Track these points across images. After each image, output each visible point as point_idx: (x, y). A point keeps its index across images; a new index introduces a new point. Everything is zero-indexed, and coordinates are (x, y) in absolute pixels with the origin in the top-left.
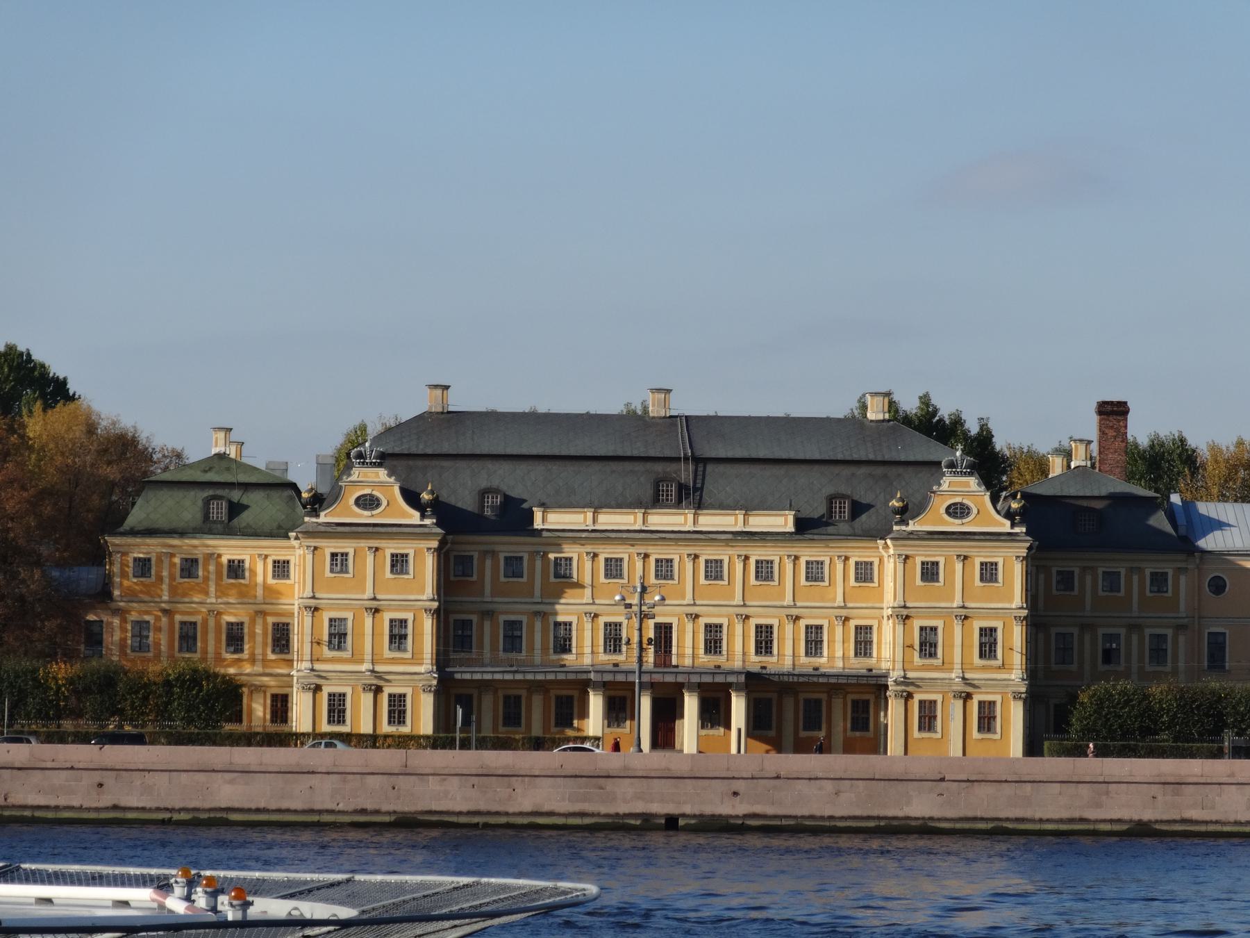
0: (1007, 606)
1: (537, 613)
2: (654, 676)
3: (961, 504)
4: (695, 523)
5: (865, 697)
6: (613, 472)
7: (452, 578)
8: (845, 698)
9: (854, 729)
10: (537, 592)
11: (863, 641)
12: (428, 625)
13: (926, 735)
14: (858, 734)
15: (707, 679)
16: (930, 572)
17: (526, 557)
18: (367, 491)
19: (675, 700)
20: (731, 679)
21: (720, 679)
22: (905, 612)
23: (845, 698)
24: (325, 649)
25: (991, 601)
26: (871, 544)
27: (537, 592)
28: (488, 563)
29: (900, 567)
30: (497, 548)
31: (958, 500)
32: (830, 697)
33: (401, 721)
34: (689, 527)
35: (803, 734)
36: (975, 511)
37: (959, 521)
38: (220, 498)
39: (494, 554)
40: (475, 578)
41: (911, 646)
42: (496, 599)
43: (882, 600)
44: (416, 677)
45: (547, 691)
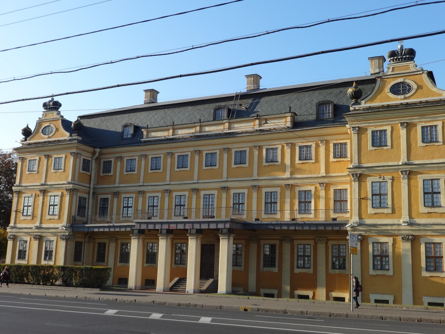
1: (140, 192)
2: (171, 225)
7: (101, 174)
8: (327, 244)
11: (340, 201)
14: (337, 271)
16: (379, 140)
19: (213, 245)
20: (221, 226)
22: (359, 171)
23: (327, 244)
25: (433, 158)
27: (142, 180)
28: (119, 163)
30: (123, 155)
31: (400, 80)
32: (316, 244)
33: (50, 259)
35: (297, 271)
36: (415, 87)
37: (402, 97)
39: (121, 158)
40: (112, 173)
41: (366, 199)
42: (121, 185)
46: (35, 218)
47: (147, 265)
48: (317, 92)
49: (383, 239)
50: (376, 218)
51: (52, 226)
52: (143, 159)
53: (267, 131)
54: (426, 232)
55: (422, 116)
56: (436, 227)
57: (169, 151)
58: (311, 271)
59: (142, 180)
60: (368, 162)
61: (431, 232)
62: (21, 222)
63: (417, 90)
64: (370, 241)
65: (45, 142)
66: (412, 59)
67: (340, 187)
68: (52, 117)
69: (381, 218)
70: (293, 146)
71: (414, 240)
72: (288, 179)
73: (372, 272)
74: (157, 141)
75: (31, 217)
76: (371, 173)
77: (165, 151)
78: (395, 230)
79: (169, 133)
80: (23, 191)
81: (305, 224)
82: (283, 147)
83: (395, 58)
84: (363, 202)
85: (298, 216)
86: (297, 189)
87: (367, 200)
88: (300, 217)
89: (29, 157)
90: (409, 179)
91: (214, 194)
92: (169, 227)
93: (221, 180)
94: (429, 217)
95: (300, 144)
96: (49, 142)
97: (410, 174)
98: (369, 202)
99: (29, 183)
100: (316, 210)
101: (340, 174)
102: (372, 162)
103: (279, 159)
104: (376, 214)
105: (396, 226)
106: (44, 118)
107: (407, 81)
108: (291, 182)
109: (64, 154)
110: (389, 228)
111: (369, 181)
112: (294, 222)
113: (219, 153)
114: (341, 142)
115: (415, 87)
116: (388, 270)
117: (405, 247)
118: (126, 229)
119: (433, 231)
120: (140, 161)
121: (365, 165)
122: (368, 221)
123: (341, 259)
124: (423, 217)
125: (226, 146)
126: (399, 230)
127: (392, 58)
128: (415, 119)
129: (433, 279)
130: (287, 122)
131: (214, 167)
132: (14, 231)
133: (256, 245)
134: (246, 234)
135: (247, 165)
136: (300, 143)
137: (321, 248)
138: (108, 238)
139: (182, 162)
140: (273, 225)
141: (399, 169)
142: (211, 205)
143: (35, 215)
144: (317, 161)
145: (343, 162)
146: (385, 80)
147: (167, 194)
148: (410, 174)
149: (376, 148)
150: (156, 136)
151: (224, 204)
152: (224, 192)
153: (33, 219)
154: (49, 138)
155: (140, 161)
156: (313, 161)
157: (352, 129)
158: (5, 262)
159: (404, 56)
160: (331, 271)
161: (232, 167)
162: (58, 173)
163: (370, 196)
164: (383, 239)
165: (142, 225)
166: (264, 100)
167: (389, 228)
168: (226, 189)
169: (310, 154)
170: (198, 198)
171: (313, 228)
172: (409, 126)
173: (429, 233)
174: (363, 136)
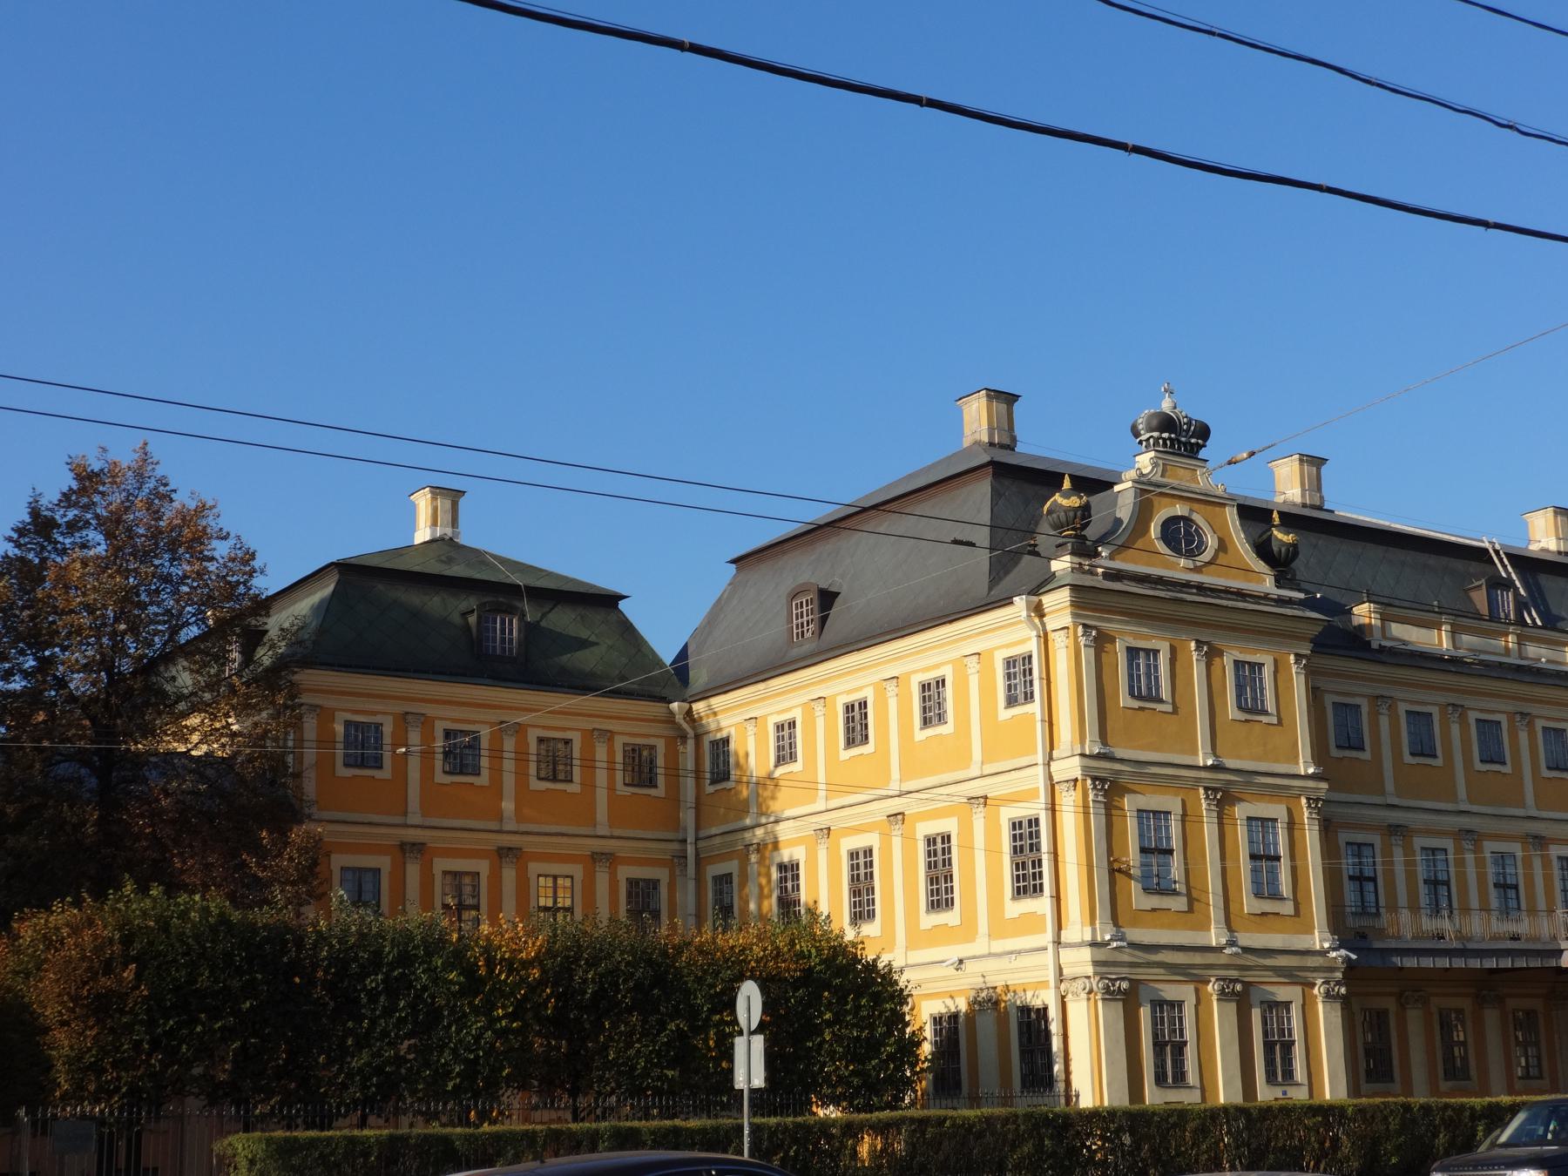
12: (1311, 837)
18: (1179, 509)
24: (1135, 887)
38: (511, 611)
44: (1311, 962)
46: (1196, 905)
47: (1450, 1084)
51: (1275, 940)
59: (977, 754)
62: (1139, 918)
65: (1187, 585)
68: (1193, 486)
75: (1184, 900)
89: (1123, 633)
96: (1201, 588)
99: (1141, 748)
106: (1158, 478)
109: (1268, 652)
120: (1374, 715)
132: (1126, 958)
143: (1195, 894)
153: (1191, 910)
154: (1197, 570)
155: (1374, 715)
158: (1143, 1101)
162: (1257, 727)
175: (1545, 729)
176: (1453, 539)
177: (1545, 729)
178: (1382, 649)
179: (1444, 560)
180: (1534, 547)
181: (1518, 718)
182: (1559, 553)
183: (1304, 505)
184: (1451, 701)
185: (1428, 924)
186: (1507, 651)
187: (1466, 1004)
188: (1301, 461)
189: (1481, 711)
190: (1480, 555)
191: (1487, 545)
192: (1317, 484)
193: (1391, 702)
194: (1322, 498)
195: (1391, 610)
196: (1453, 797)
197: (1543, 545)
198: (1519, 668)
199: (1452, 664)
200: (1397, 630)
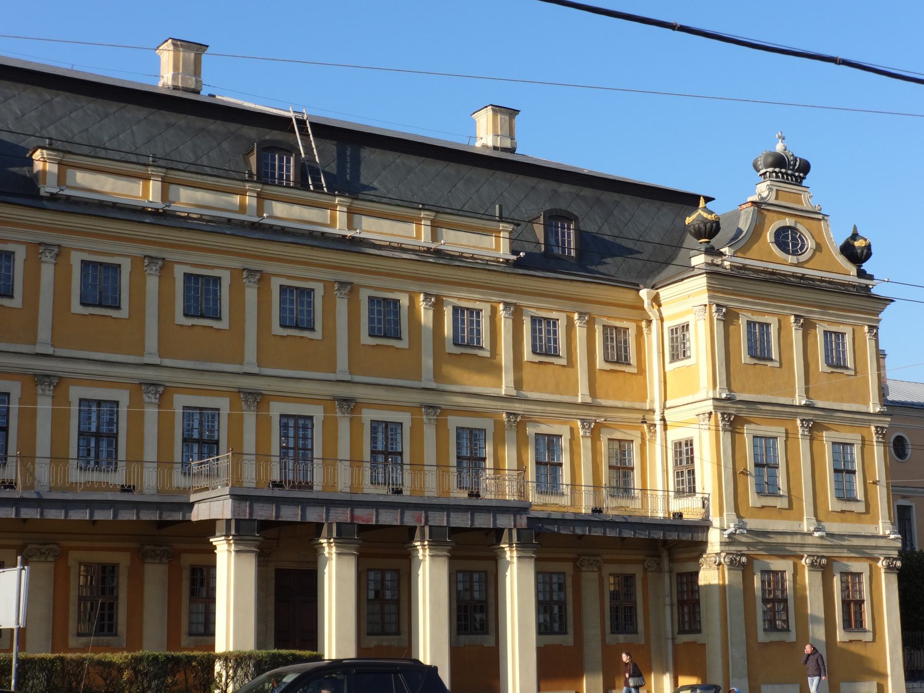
0: (863, 409)
1: (41, 378)
3: (794, 229)
4: (350, 226)
5: (629, 569)
6: (169, 126)
8: (600, 569)
9: (617, 629)
10: (44, 333)
13: (775, 637)
15: (460, 520)
17: (20, 254)
21: (483, 521)
25: (842, 400)
26: (625, 295)
27: (44, 333)
29: (718, 328)
31: (788, 222)
32: (577, 570)
34: (340, 227)
41: (745, 473)
43: (644, 398)
45: (60, 557)
48: (499, 174)
49: (777, 564)
50: (765, 518)
52: (48, 257)
53: (452, 257)
54: (836, 550)
55: (824, 307)
56: (856, 542)
57: (153, 251)
58: (568, 640)
60: (743, 390)
61: (845, 550)
63: (815, 251)
64: (757, 566)
66: (799, 181)
67: (618, 435)
69: (770, 518)
70: (517, 314)
71: (825, 568)
72: (508, 399)
73: (762, 637)
74: (101, 205)
76: (753, 416)
77: (138, 251)
78: (796, 545)
79: (146, 190)
80: (825, 422)
81: (627, 523)
82: (494, 311)
83: (783, 170)
84: (740, 478)
85: (533, 497)
86: (531, 430)
87: (747, 475)
88: (613, 507)
90: (812, 439)
91: (311, 418)
92: (352, 517)
93: (331, 376)
94: (843, 521)
95: (534, 310)
97: (814, 429)
98: (751, 481)
100: (574, 485)
101: (619, 404)
102: (749, 392)
103: (485, 342)
104: (763, 507)
105: (799, 537)
107: (799, 227)
108: (518, 407)
110: (788, 539)
111: (748, 432)
112: (597, 517)
113: (322, 293)
114: (617, 324)
115: (810, 244)
116: (788, 630)
117: (810, 580)
118: (115, 515)
119: (851, 548)
121: (740, 397)
122: (753, 524)
123: (556, 609)
124: (833, 521)
125: (344, 277)
126: (803, 545)
127: (777, 170)
128: (814, 312)
129: (853, 648)
130: (497, 245)
131: (307, 334)
133: (595, 575)
134: (560, 545)
135: (404, 344)
136: (534, 308)
137: (590, 578)
138: (642, 562)
139: (202, 296)
140: (556, 521)
141: (797, 414)
142: (296, 448)
144: (571, 363)
145: (622, 374)
146: (765, 213)
147: (150, 398)
148: (814, 429)
149: (756, 362)
150: (96, 187)
151: (344, 451)
152: (249, 406)
156: (564, 362)
157: (714, 308)
159: (796, 171)
160: (610, 639)
161: (362, 342)
163: (750, 467)
164: (777, 564)
165: (256, 506)
166: (368, 155)
167: (788, 539)
168: (349, 404)
169: (555, 341)
170: (263, 424)
171: (644, 535)
172: (807, 326)
173: (845, 553)
174: (732, 327)
175: (283, 289)
176: (232, 100)
177: (283, 289)
178: (53, 197)
179: (233, 127)
180: (478, 144)
181: (245, 274)
182: (495, 148)
183: (176, 88)
184: (246, 266)
185: (76, 476)
186: (242, 208)
187: (123, 560)
188: (175, 45)
189: (90, 252)
190: (283, 123)
191: (291, 114)
192: (197, 72)
193: (61, 253)
194: (198, 82)
195: (173, 174)
196: (140, 349)
197: (484, 141)
198: (254, 226)
199: (162, 217)
200: (83, 178)
